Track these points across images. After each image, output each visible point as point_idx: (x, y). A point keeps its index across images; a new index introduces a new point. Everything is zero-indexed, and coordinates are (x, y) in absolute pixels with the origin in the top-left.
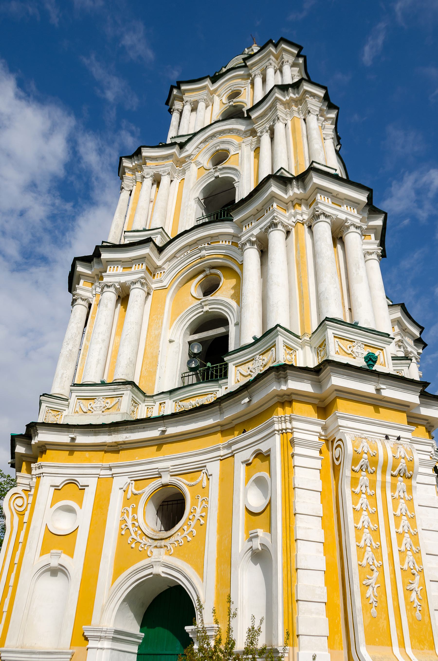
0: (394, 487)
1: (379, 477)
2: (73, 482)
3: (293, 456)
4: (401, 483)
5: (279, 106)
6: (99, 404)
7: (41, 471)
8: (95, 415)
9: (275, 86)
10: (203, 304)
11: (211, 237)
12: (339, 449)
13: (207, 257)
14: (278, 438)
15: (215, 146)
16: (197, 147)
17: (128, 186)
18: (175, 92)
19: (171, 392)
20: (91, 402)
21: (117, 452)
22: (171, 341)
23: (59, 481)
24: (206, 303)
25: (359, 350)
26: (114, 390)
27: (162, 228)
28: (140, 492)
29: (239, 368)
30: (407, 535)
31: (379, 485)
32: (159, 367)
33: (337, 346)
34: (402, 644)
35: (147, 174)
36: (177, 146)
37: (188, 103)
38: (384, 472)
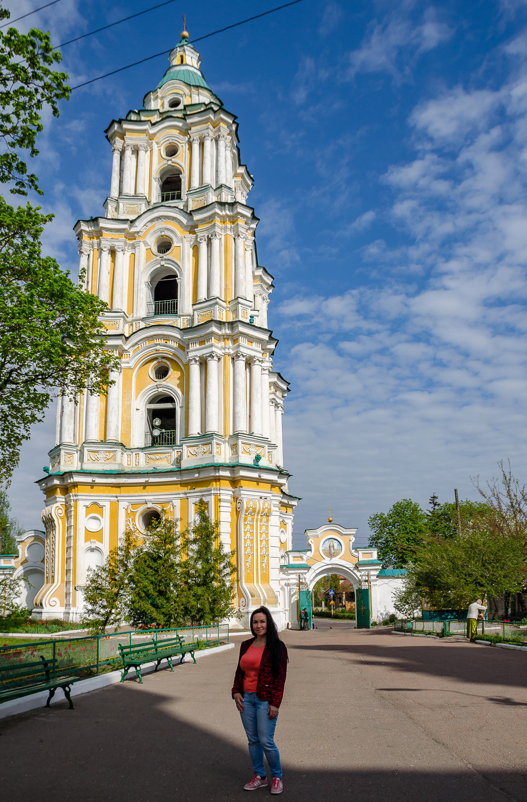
0: (261, 521)
1: (256, 517)
2: (96, 503)
3: (220, 506)
4: (264, 519)
5: (217, 221)
6: (101, 456)
7: (77, 498)
8: (101, 463)
9: (216, 202)
10: (158, 386)
11: (164, 335)
12: (239, 504)
13: (160, 351)
14: (213, 497)
15: (162, 230)
16: (145, 225)
17: (86, 251)
18: (116, 126)
19: (142, 449)
20: (97, 454)
21: (119, 487)
22: (137, 410)
23: (88, 503)
24: (161, 386)
25: (253, 450)
26: (111, 448)
27: (124, 312)
28: (135, 510)
29: (189, 448)
30: (264, 541)
31: (255, 520)
32: (132, 428)
33: (243, 449)
34: (258, 582)
35: (105, 247)
36: (129, 222)
37: (130, 148)
38: (258, 514)
